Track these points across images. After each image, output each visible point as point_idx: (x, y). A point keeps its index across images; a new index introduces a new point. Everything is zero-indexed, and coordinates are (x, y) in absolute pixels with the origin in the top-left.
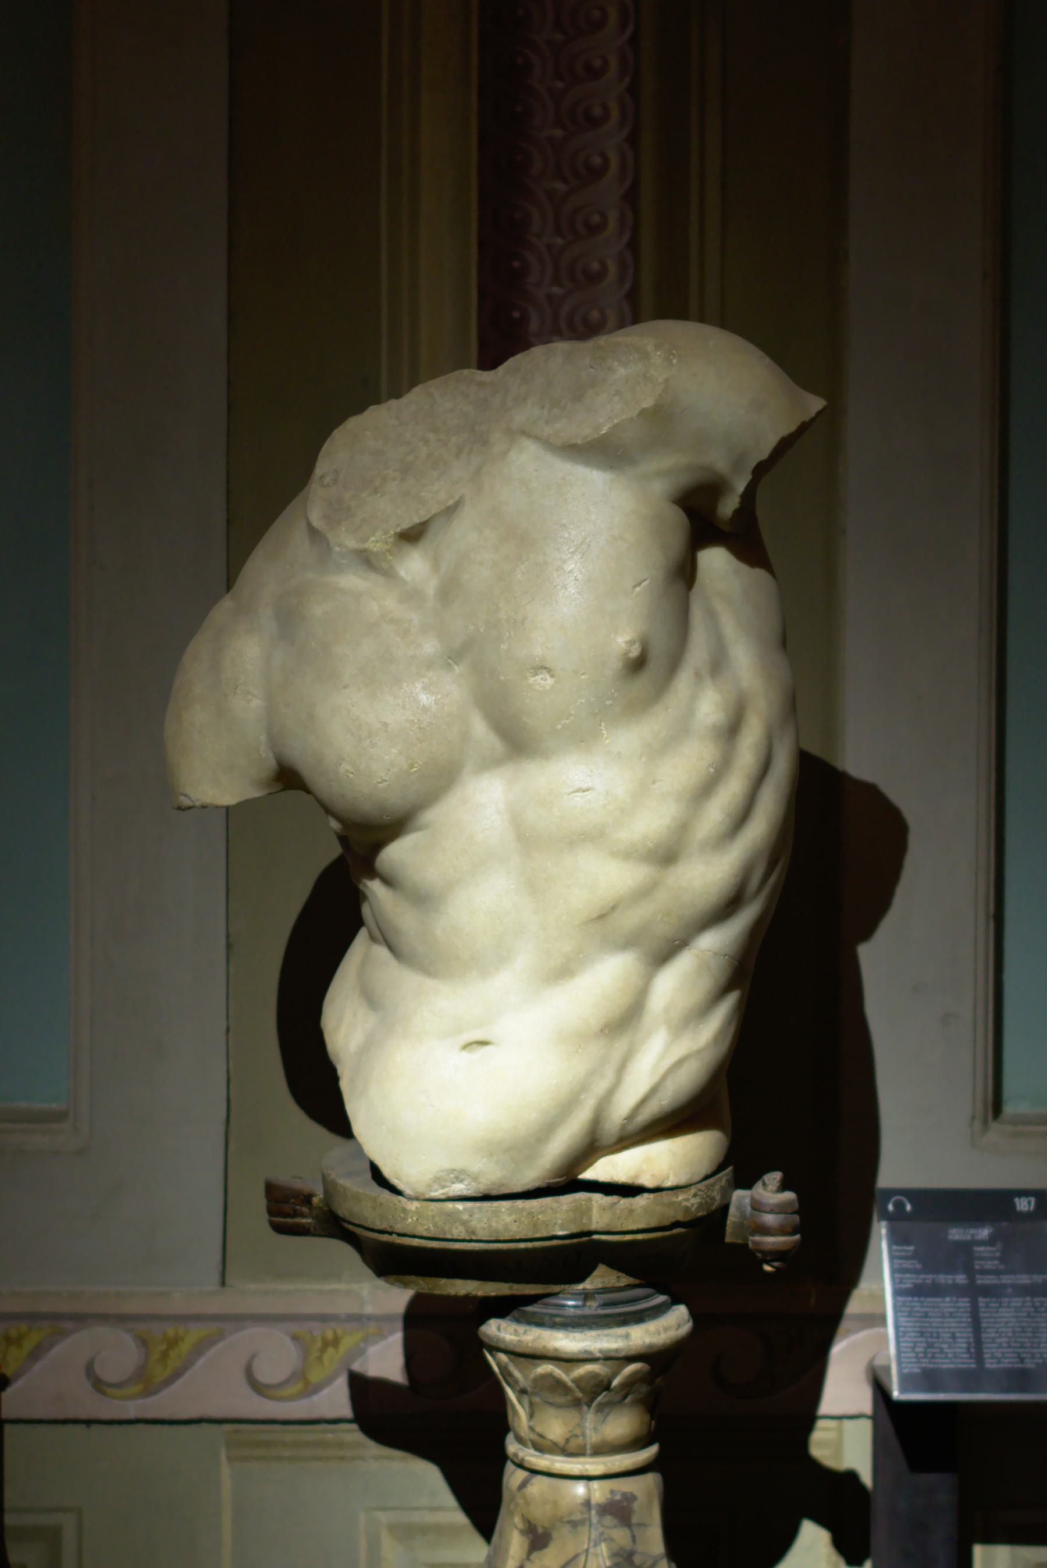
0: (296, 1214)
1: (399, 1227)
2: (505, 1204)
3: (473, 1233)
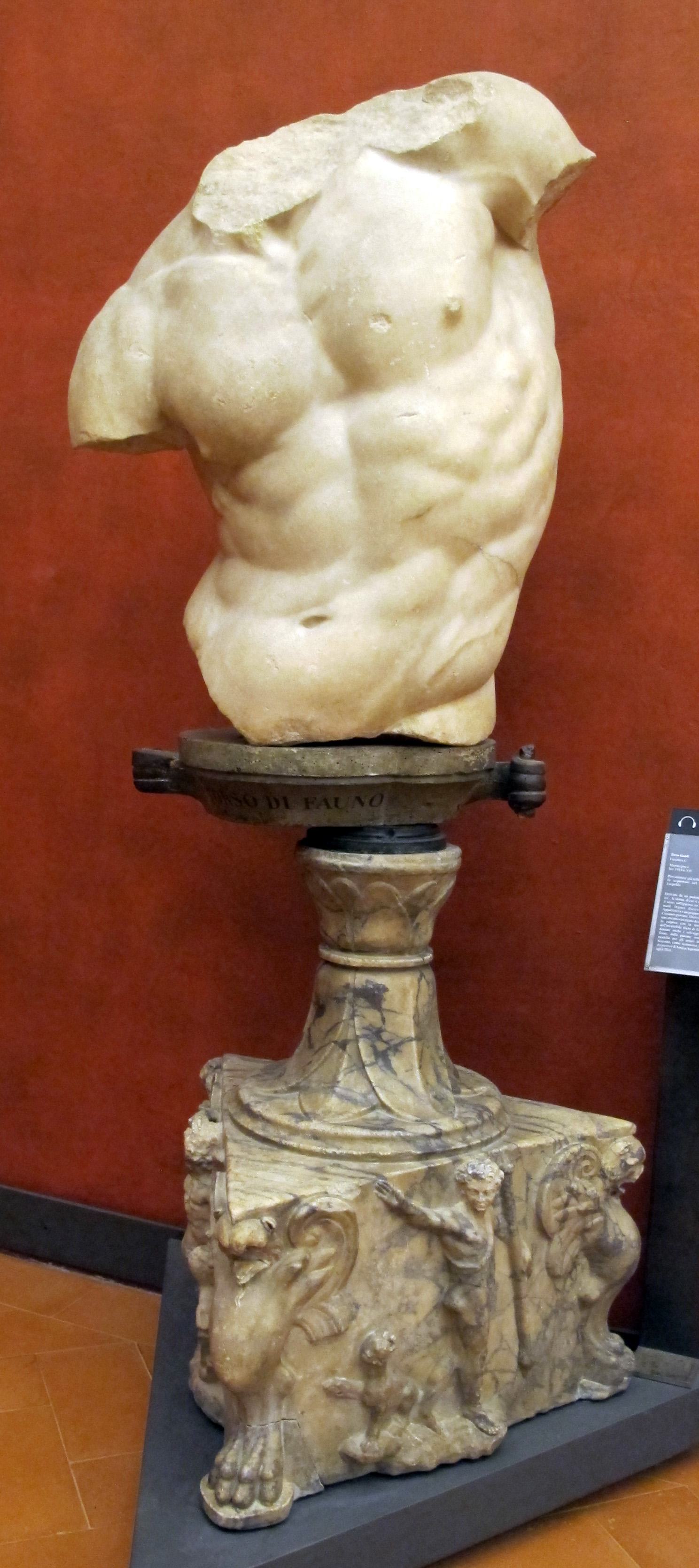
0: (155, 775)
1: (244, 768)
2: (329, 751)
3: (304, 771)
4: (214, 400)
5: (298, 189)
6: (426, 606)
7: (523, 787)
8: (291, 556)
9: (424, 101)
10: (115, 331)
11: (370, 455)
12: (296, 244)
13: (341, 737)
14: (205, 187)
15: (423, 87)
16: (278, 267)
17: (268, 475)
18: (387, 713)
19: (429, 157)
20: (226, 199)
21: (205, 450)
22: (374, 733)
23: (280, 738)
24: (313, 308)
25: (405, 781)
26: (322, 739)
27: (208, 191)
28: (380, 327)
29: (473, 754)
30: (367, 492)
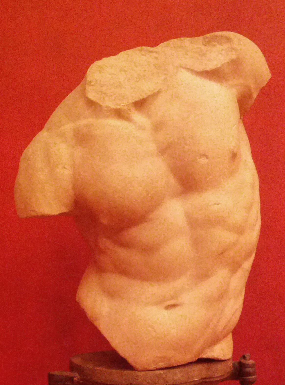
2: (177, 370)
3: (167, 382)
4: (116, 196)
5: (147, 87)
6: (222, 296)
7: (249, 374)
8: (158, 274)
9: (204, 45)
10: (48, 157)
11: (198, 224)
12: (149, 116)
13: (183, 363)
14: (91, 82)
15: (201, 38)
16: (142, 128)
17: (142, 233)
18: (203, 350)
19: (214, 75)
20: (104, 89)
21: (105, 221)
22: (195, 359)
23: (154, 367)
24: (163, 150)
25: (207, 380)
26: (174, 365)
27: (92, 84)
28: (203, 161)
30: (197, 243)
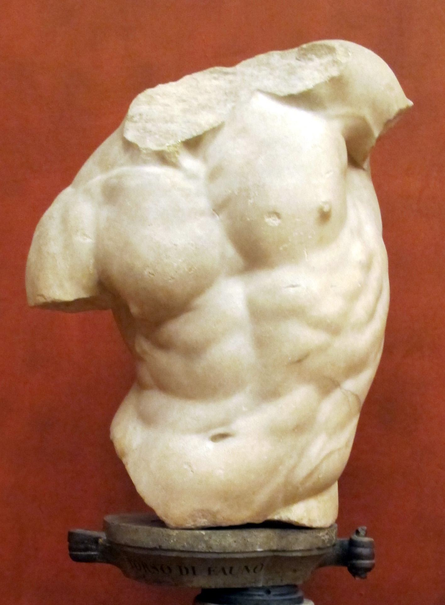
0: (87, 549)
1: (164, 546)
2: (229, 533)
3: (211, 548)
4: (146, 273)
5: (206, 120)
6: (301, 427)
8: (203, 388)
9: (297, 59)
10: (65, 221)
11: (264, 317)
12: (205, 160)
13: (238, 523)
14: (133, 117)
15: (296, 50)
16: (192, 176)
17: (184, 328)
18: (271, 505)
19: (305, 100)
20: (149, 126)
21: (134, 310)
22: (260, 520)
23: (192, 523)
24: (220, 207)
25: (281, 554)
26: (224, 525)
28: (273, 222)
29: (327, 534)
30: (261, 343)
